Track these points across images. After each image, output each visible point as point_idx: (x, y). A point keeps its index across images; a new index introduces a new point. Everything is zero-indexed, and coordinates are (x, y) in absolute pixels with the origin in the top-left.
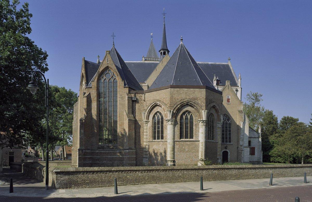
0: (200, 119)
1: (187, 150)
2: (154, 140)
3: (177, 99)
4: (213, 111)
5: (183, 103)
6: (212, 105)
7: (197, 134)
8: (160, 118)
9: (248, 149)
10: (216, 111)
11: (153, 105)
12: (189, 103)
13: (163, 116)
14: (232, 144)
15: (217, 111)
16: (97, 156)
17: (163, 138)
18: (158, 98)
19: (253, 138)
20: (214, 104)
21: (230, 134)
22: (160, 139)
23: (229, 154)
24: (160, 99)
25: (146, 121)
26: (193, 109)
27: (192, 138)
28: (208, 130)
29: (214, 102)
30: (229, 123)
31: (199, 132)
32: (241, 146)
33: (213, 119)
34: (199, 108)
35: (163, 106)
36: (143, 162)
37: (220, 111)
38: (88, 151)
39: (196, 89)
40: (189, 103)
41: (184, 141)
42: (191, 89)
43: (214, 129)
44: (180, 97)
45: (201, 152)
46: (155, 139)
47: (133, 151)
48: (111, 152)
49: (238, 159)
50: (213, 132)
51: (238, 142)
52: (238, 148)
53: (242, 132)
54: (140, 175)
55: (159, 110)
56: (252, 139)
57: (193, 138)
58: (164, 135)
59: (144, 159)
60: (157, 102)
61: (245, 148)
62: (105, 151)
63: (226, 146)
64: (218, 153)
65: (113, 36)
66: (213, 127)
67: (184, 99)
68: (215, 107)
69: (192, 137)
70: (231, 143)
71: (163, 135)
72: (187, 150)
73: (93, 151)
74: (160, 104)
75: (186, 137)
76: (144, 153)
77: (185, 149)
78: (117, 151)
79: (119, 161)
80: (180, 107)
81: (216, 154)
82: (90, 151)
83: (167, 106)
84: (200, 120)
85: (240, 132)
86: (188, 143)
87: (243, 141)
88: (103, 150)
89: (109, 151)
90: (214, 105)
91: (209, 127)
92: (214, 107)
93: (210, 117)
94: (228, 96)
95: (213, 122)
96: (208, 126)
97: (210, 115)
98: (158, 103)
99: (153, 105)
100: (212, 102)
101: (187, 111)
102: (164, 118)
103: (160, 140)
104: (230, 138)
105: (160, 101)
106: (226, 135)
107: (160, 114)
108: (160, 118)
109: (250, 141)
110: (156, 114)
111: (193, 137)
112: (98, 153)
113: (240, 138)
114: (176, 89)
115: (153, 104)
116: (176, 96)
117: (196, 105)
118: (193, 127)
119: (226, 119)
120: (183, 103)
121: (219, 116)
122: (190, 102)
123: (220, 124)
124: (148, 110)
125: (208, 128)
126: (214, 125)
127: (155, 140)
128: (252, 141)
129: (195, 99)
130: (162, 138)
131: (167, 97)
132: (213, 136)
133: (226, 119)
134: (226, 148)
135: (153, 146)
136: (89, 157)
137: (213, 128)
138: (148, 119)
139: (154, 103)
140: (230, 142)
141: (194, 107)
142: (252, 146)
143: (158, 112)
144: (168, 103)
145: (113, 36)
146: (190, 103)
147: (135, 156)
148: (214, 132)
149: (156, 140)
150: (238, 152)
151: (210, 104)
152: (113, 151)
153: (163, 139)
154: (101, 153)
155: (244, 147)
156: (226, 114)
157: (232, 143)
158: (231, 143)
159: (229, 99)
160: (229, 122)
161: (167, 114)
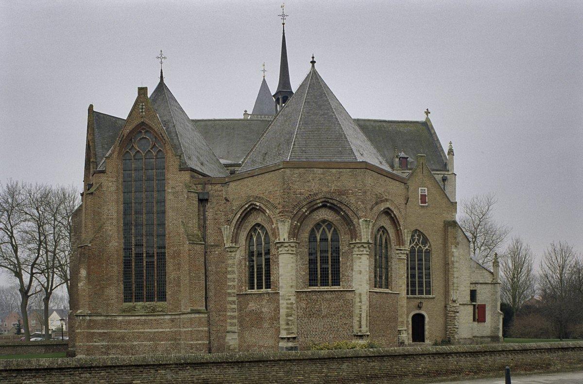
0: (355, 241)
1: (324, 312)
2: (249, 291)
3: (301, 194)
4: (385, 222)
5: (315, 203)
6: (382, 207)
7: (348, 276)
9: (470, 309)
10: (394, 220)
11: (247, 208)
12: (328, 202)
13: (270, 234)
14: (434, 298)
15: (395, 222)
16: (120, 328)
17: (270, 285)
18: (256, 194)
19: (481, 284)
20: (388, 205)
21: (428, 275)
22: (264, 287)
23: (427, 320)
24: (261, 196)
25: (231, 247)
26: (338, 218)
27: (337, 285)
28: (375, 267)
29: (387, 200)
30: (427, 249)
31: (352, 270)
32: (454, 301)
33: (386, 240)
34: (350, 214)
35: (267, 211)
36: (226, 341)
37: (401, 223)
38: (99, 318)
39: (344, 170)
40: (328, 202)
41: (319, 292)
42: (331, 170)
43: (389, 263)
44: (307, 189)
45: (359, 316)
46: (252, 288)
47: (202, 315)
48: (152, 320)
49: (447, 331)
50: (387, 269)
51: (447, 293)
52: (446, 307)
53: (455, 270)
54: (169, 377)
56: (478, 288)
57: (339, 285)
58: (272, 278)
59: (228, 334)
60: (255, 203)
61: (462, 307)
62: (137, 318)
63: (421, 303)
64: (400, 319)
65: (161, 57)
66: (387, 258)
67: (316, 194)
68: (390, 212)
69: (336, 282)
70: (431, 296)
71: (270, 279)
72: (324, 312)
73: (110, 318)
74: (262, 206)
75: (324, 283)
76: (229, 321)
77: (320, 311)
78: (166, 317)
79: (171, 340)
80: (306, 211)
81: (395, 319)
82: (103, 318)
83: (278, 211)
84: (354, 242)
85: (450, 270)
86: (328, 296)
87: (458, 290)
88: (132, 316)
89: (146, 318)
90: (388, 208)
91: (378, 257)
92: (387, 212)
93: (379, 236)
94: (422, 188)
95: (386, 247)
96: (376, 256)
97: (379, 230)
98: (258, 204)
99: (245, 210)
100: (382, 201)
101: (324, 221)
102: (272, 238)
103: (264, 290)
104: (428, 284)
106: (419, 277)
107: (263, 228)
109: (475, 290)
111: (339, 282)
112: (121, 322)
113: (450, 283)
114: (297, 171)
115: (247, 206)
116: (296, 187)
117: (343, 207)
118: (339, 259)
119: (419, 240)
120: (315, 203)
121: (398, 233)
122: (330, 201)
123: (402, 252)
124: (234, 222)
125: (376, 260)
126: (389, 253)
127: (253, 290)
128: (478, 292)
129: (341, 193)
131: (276, 189)
132: (387, 279)
133: (419, 240)
134: (419, 307)
135: (248, 304)
136: (100, 331)
137: (387, 262)
138: (236, 242)
139: (249, 204)
140: (428, 292)
141: (338, 213)
142: (478, 303)
143: (258, 225)
144: (279, 204)
145: (161, 57)
146: (331, 204)
147: (207, 328)
148: (389, 269)
149: (255, 291)
150: (446, 316)
151: (377, 204)
152: (155, 318)
153: (270, 288)
154: (129, 322)
155: (460, 305)
156: (418, 230)
157: (434, 296)
158: (431, 296)
159: (425, 196)
160: (427, 247)
161: (278, 229)
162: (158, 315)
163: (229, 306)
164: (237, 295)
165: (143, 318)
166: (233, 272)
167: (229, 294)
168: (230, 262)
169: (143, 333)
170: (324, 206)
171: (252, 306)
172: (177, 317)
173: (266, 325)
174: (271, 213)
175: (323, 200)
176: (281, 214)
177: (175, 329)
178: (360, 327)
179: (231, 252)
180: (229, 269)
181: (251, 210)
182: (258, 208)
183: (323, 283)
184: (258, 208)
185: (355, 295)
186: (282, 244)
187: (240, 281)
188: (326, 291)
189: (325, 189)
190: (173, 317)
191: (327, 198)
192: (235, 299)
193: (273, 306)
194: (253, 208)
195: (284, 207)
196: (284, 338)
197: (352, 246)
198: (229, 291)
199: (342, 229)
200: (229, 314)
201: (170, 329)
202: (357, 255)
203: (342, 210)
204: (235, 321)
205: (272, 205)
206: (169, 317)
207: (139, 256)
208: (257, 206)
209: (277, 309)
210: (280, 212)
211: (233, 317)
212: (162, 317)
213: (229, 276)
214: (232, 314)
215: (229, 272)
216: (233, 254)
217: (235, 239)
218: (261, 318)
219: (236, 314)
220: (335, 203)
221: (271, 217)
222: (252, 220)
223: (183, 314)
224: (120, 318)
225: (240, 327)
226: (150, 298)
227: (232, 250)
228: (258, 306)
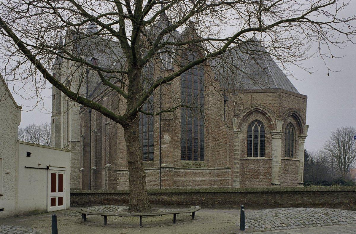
2: (249, 158)
3: (286, 107)
8: (259, 128)
16: (182, 177)
34: (301, 121)
48: (199, 172)
55: (258, 118)
60: (259, 108)
62: (192, 171)
67: (291, 109)
77: (288, 170)
83: (276, 115)
86: (291, 162)
98: (261, 109)
103: (259, 157)
105: (264, 107)
107: (260, 122)
108: (259, 128)
110: (253, 123)
115: (252, 109)
117: (300, 117)
122: (296, 113)
124: (242, 117)
130: (262, 155)
131: (274, 102)
135: (249, 165)
143: (256, 120)
152: (201, 171)
154: (187, 173)
162: (203, 169)
163: (235, 166)
164: (240, 159)
165: (195, 171)
166: (238, 146)
167: (235, 159)
168: (236, 140)
169: (194, 181)
170: (292, 116)
171: (252, 166)
172: (213, 171)
173: (261, 177)
174: (271, 115)
175: (293, 112)
176: (277, 117)
177: (212, 179)
178: (302, 179)
179: (238, 134)
180: (236, 144)
181: (254, 112)
182: (261, 111)
183: (249, 155)
184: (261, 111)
185: (299, 163)
186: (278, 133)
187: (242, 151)
188: (291, 160)
189: (294, 107)
190: (210, 171)
191: (295, 112)
192: (238, 161)
193: (267, 167)
194: (256, 111)
195: (279, 113)
196: (277, 184)
197: (299, 138)
198: (236, 157)
199: (297, 128)
200: (235, 170)
201: (209, 178)
202: (302, 142)
203: (299, 119)
204: (238, 174)
205: (272, 111)
206: (208, 171)
207: (256, 137)
208: (260, 110)
209: (270, 168)
210: (277, 116)
211: (237, 172)
212: (205, 171)
213: (235, 148)
214: (237, 170)
215: (235, 146)
216: (238, 135)
217: (240, 127)
218: (258, 173)
219: (239, 170)
220: (297, 115)
221: (271, 117)
222: (253, 118)
223: (218, 169)
224: (182, 171)
225: (241, 178)
226: (196, 159)
227: (239, 133)
228: (256, 166)
